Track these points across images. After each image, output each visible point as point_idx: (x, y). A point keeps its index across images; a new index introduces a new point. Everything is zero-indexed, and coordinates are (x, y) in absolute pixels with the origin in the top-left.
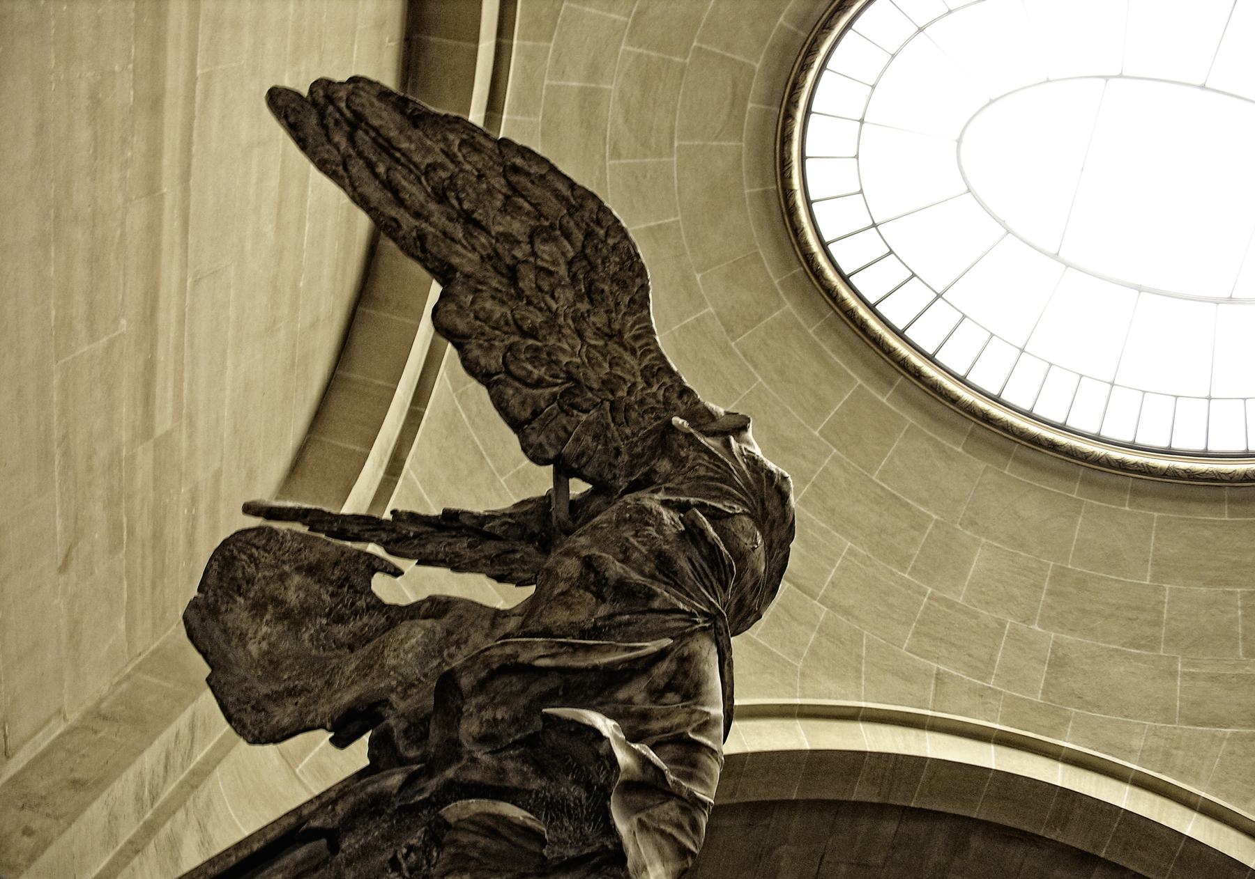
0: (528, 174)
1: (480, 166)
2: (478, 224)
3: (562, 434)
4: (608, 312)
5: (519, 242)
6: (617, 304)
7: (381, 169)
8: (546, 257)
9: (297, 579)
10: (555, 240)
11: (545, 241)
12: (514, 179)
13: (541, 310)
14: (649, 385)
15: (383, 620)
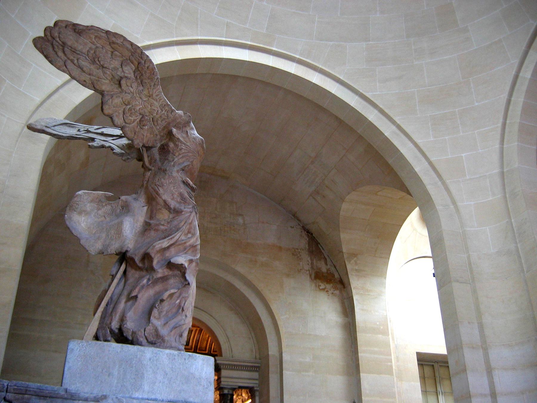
0: (118, 44)
1: (102, 44)
2: (106, 68)
3: (142, 137)
4: (148, 89)
5: (118, 69)
6: (151, 86)
7: (76, 62)
8: (127, 72)
9: (89, 204)
10: (128, 64)
11: (126, 66)
12: (113, 46)
13: (129, 94)
14: (162, 110)
15: (110, 207)
